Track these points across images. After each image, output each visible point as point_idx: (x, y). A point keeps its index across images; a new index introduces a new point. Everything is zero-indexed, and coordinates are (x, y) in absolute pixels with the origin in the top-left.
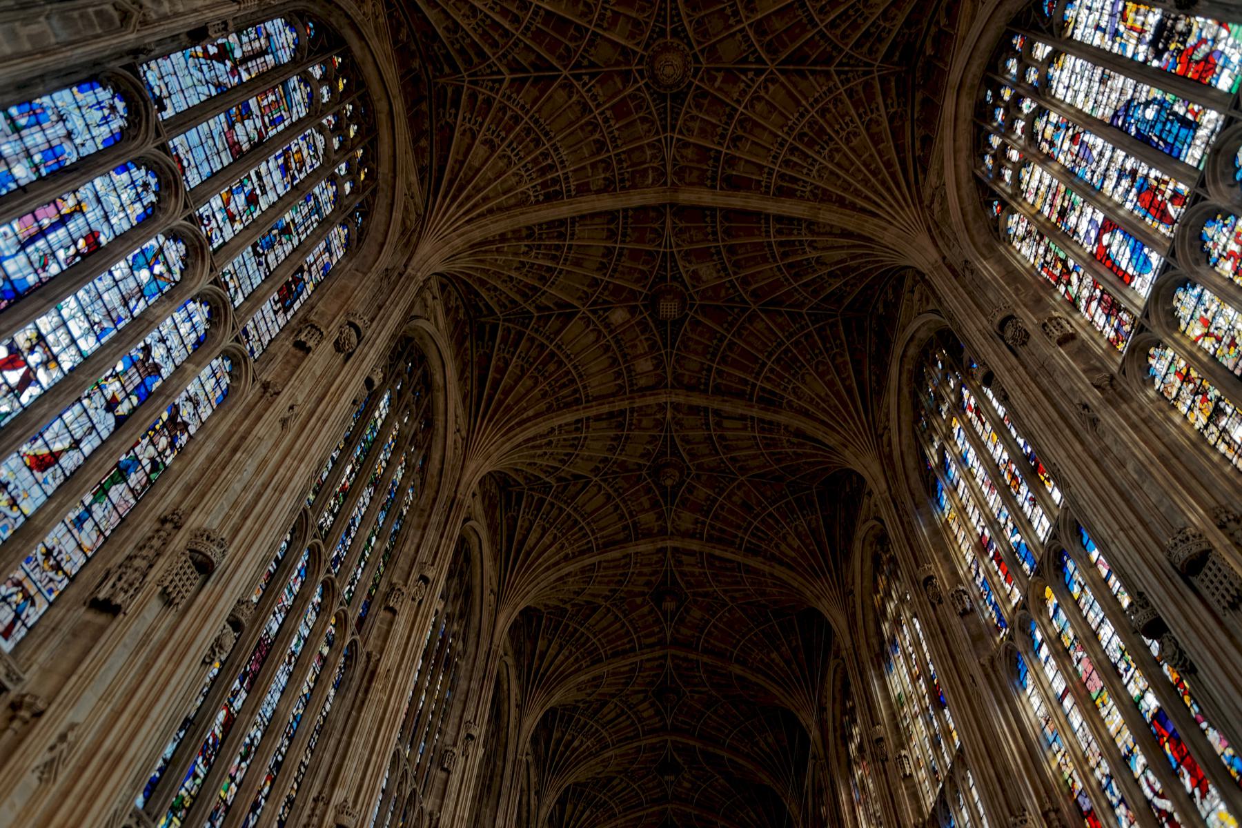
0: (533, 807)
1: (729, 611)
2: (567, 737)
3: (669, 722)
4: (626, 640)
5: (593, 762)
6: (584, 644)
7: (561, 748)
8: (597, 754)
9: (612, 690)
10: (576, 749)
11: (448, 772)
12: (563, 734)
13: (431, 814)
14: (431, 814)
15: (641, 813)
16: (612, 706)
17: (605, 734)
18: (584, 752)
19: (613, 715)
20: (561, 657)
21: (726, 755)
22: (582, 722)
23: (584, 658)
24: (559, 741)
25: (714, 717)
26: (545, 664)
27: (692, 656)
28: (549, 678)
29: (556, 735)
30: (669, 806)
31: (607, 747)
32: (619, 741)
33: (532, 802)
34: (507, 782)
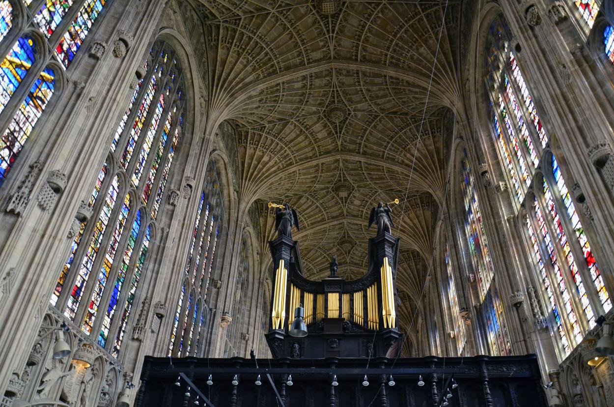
0: (232, 198)
1: (382, 11)
2: (258, 153)
3: (339, 143)
4: (295, 52)
5: (281, 175)
6: (259, 54)
7: (254, 162)
8: (284, 169)
9: (289, 107)
10: (267, 163)
11: (97, 59)
12: (255, 149)
13: (75, 84)
14: (75, 84)
15: (325, 226)
16: (292, 127)
17: (288, 152)
18: (273, 166)
19: (293, 135)
20: (239, 66)
21: (385, 165)
22: (269, 141)
23: (260, 67)
24: (252, 158)
25: (375, 133)
26: (226, 70)
27: (353, 67)
28: (232, 82)
29: (249, 152)
30: (345, 221)
31: (291, 164)
32: (301, 160)
33: (232, 194)
34: (195, 150)
